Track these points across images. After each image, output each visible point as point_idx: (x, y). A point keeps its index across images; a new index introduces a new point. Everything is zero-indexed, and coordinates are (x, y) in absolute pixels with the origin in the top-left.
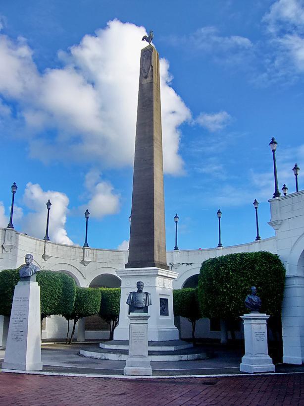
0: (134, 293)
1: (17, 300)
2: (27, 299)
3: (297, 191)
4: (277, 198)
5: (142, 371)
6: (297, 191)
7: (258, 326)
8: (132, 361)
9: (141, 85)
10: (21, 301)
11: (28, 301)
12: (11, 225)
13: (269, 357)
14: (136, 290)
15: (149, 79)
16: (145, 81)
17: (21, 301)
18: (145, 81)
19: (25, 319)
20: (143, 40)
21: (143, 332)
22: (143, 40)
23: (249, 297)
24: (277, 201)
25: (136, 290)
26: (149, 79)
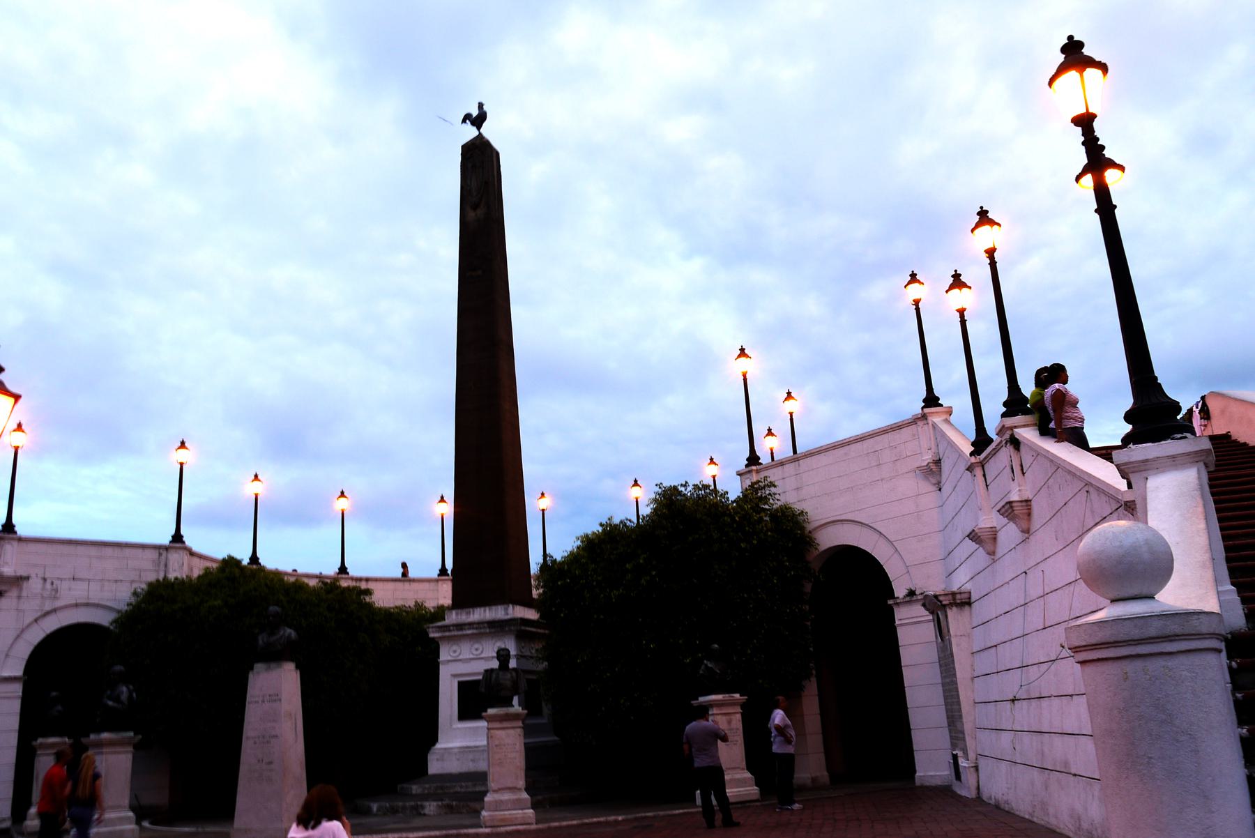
0: (492, 670)
1: (257, 699)
2: (276, 698)
3: (795, 451)
4: (754, 468)
5: (516, 818)
6: (795, 451)
7: (727, 717)
8: (496, 801)
10: (263, 701)
11: (280, 700)
12: (178, 537)
13: (748, 775)
14: (495, 664)
15: (481, 212)
16: (471, 215)
17: (263, 701)
19: (276, 736)
22: (464, 121)
23: (706, 665)
24: (754, 474)
25: (495, 664)
26: (481, 212)
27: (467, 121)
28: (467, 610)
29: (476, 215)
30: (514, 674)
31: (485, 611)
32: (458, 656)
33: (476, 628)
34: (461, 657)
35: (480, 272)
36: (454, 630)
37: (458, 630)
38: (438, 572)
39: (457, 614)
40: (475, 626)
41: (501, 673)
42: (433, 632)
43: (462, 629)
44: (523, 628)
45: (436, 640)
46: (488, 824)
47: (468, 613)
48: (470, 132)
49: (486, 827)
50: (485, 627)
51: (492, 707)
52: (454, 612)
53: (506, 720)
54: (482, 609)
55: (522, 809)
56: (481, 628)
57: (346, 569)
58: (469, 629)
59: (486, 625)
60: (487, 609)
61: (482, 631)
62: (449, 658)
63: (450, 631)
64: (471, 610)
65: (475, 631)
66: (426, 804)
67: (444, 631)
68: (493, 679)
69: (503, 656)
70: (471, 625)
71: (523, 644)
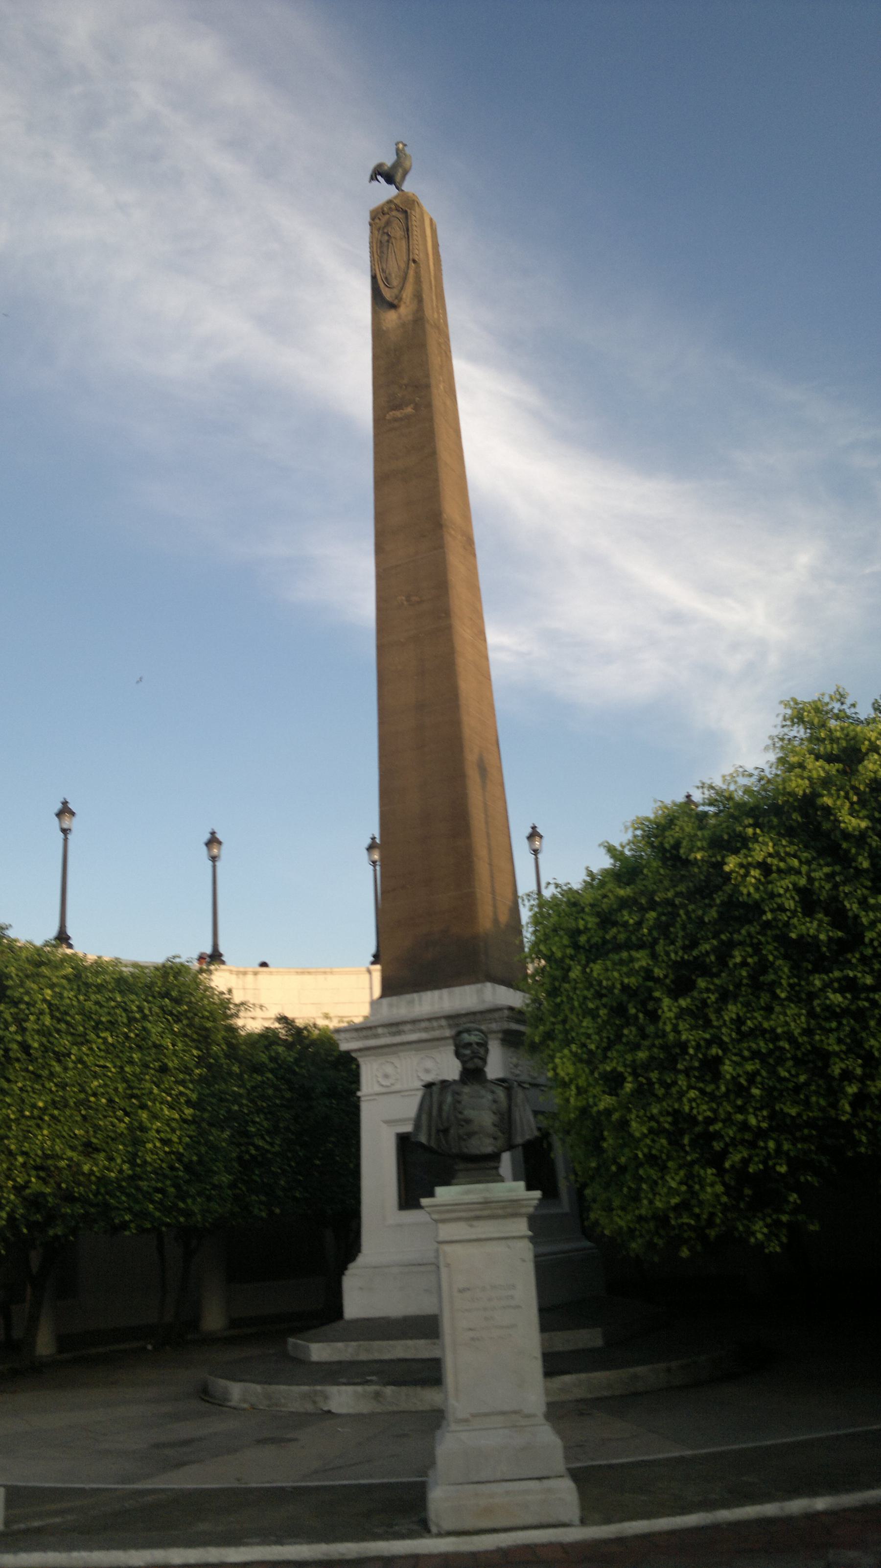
0: (444, 1084)
9: (378, 333)
15: (405, 310)
18: (391, 318)
20: (373, 178)
21: (513, 1287)
22: (373, 178)
27: (379, 178)
28: (408, 997)
29: (399, 318)
30: (501, 1094)
31: (441, 998)
32: (392, 1084)
33: (426, 1030)
34: (397, 1087)
35: (409, 410)
36: (384, 1035)
37: (394, 1034)
38: (372, 959)
39: (390, 1005)
40: (424, 1025)
41: (466, 1089)
42: (347, 1040)
43: (399, 1033)
44: (514, 1026)
45: (354, 1055)
46: (447, 1526)
47: (411, 1002)
48: (385, 192)
49: (440, 1535)
50: (441, 1027)
51: (447, 1183)
52: (385, 1001)
53: (478, 1218)
54: (436, 993)
55: (539, 1479)
56: (433, 1029)
57: (221, 955)
58: (413, 1031)
59: (443, 1022)
60: (445, 992)
61: (437, 1034)
62: (378, 1089)
63: (376, 1036)
64: (415, 996)
65: (424, 1035)
66: (333, 1390)
67: (366, 1038)
68: (446, 1108)
69: (469, 1045)
70: (414, 1022)
71: (515, 1060)
